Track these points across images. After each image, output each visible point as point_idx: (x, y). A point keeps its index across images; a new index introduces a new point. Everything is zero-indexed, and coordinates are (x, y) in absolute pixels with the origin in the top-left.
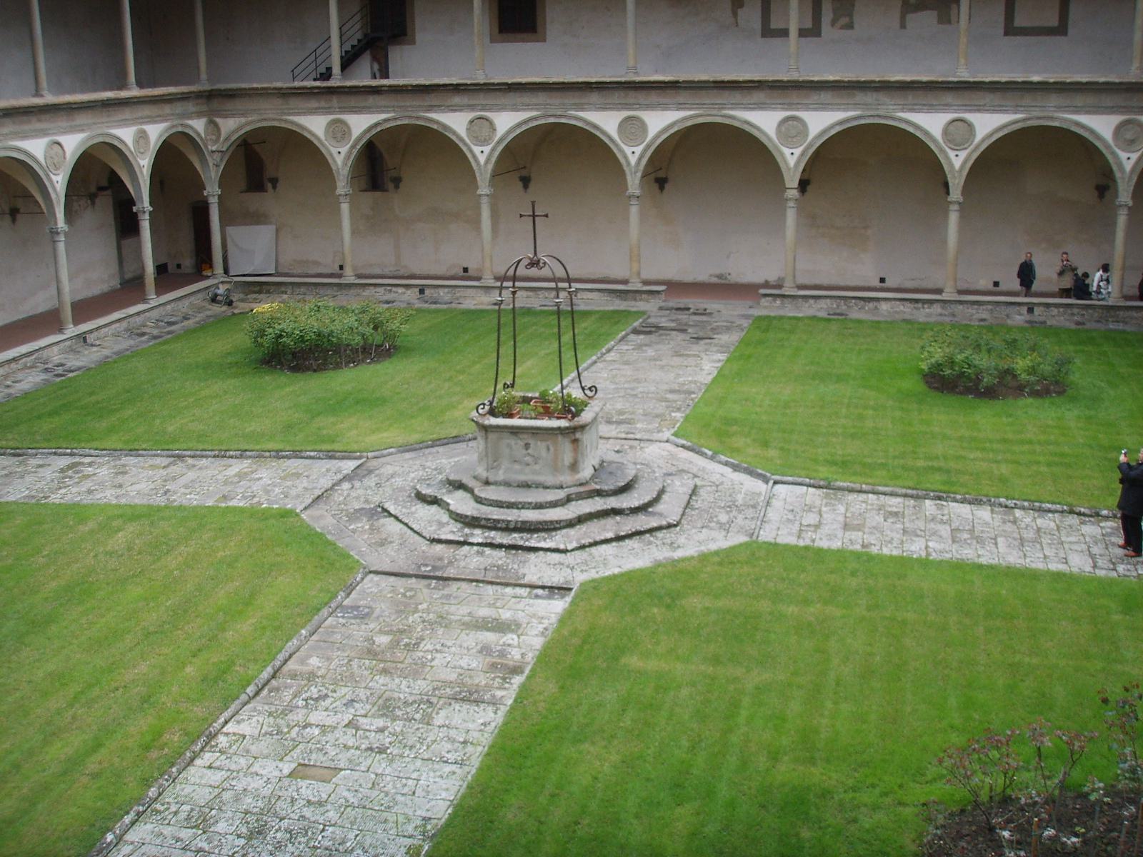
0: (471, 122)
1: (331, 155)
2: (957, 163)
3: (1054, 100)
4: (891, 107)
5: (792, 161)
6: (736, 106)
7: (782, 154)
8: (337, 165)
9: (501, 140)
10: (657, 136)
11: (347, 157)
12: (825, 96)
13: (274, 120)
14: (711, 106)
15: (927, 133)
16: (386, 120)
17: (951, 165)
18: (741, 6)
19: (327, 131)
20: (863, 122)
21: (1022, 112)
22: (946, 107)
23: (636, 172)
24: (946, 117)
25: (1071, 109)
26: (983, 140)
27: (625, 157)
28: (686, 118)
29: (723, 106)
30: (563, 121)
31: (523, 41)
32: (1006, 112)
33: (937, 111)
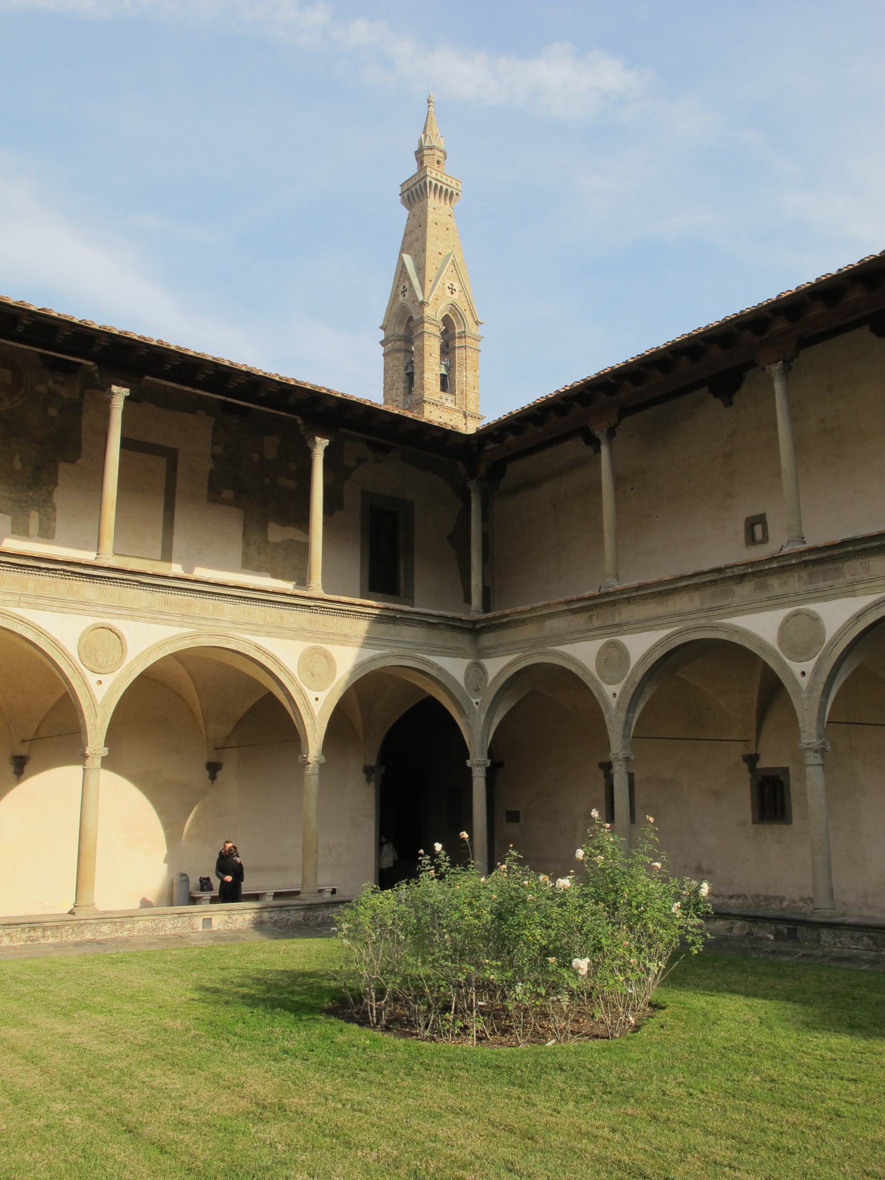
2: (100, 694)
3: (230, 610)
15: (55, 643)
17: (92, 697)
22: (84, 606)
26: (137, 659)
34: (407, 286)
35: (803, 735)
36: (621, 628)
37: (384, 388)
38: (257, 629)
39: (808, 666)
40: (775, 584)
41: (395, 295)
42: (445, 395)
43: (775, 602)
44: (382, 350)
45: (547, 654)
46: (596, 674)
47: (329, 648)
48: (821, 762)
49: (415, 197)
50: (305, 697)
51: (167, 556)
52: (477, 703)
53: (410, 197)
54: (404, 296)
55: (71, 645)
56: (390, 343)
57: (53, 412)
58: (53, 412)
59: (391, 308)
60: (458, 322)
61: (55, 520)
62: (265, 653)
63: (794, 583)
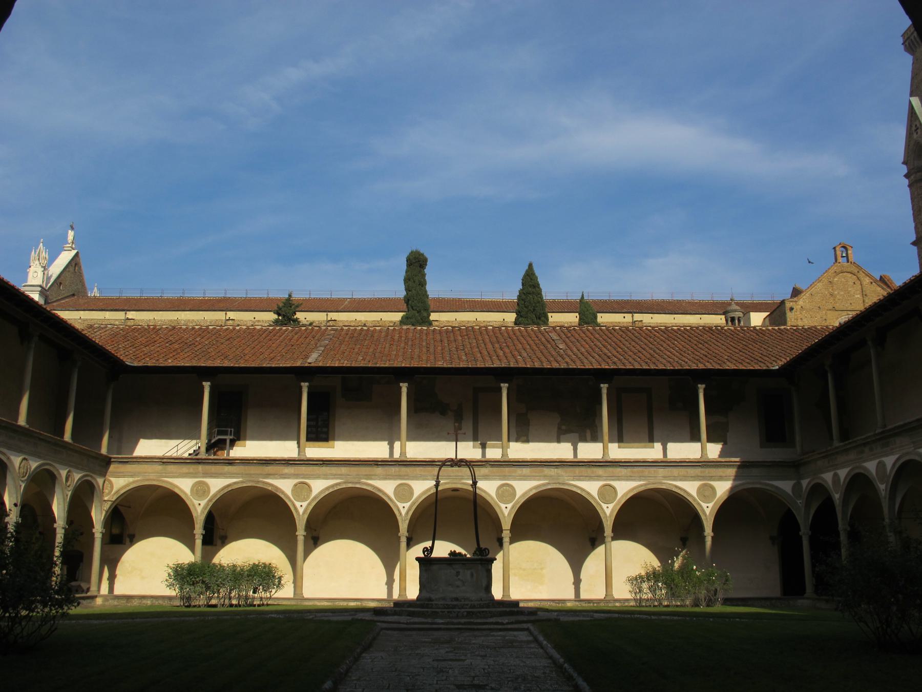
0: (295, 485)
1: (194, 505)
2: (608, 512)
4: (566, 478)
5: (506, 512)
7: (500, 507)
8: (197, 512)
9: (315, 498)
10: (419, 497)
11: (204, 508)
12: (526, 471)
13: (154, 480)
14: (454, 477)
15: (589, 493)
16: (235, 483)
17: (605, 513)
19: (192, 490)
20: (549, 487)
21: (643, 480)
22: (598, 478)
23: (405, 520)
24: (599, 484)
25: (672, 478)
26: (622, 496)
27: (399, 510)
30: (358, 486)
31: (319, 447)
32: (634, 480)
33: (594, 480)
34: (918, 125)
37: (913, 214)
38: (675, 479)
41: (910, 134)
44: (906, 182)
47: (712, 483)
49: (915, 43)
50: (701, 506)
51: (651, 440)
52: (800, 503)
53: (911, 44)
54: (917, 133)
55: (595, 493)
56: (911, 175)
59: (909, 146)
61: (597, 432)
62: (680, 488)
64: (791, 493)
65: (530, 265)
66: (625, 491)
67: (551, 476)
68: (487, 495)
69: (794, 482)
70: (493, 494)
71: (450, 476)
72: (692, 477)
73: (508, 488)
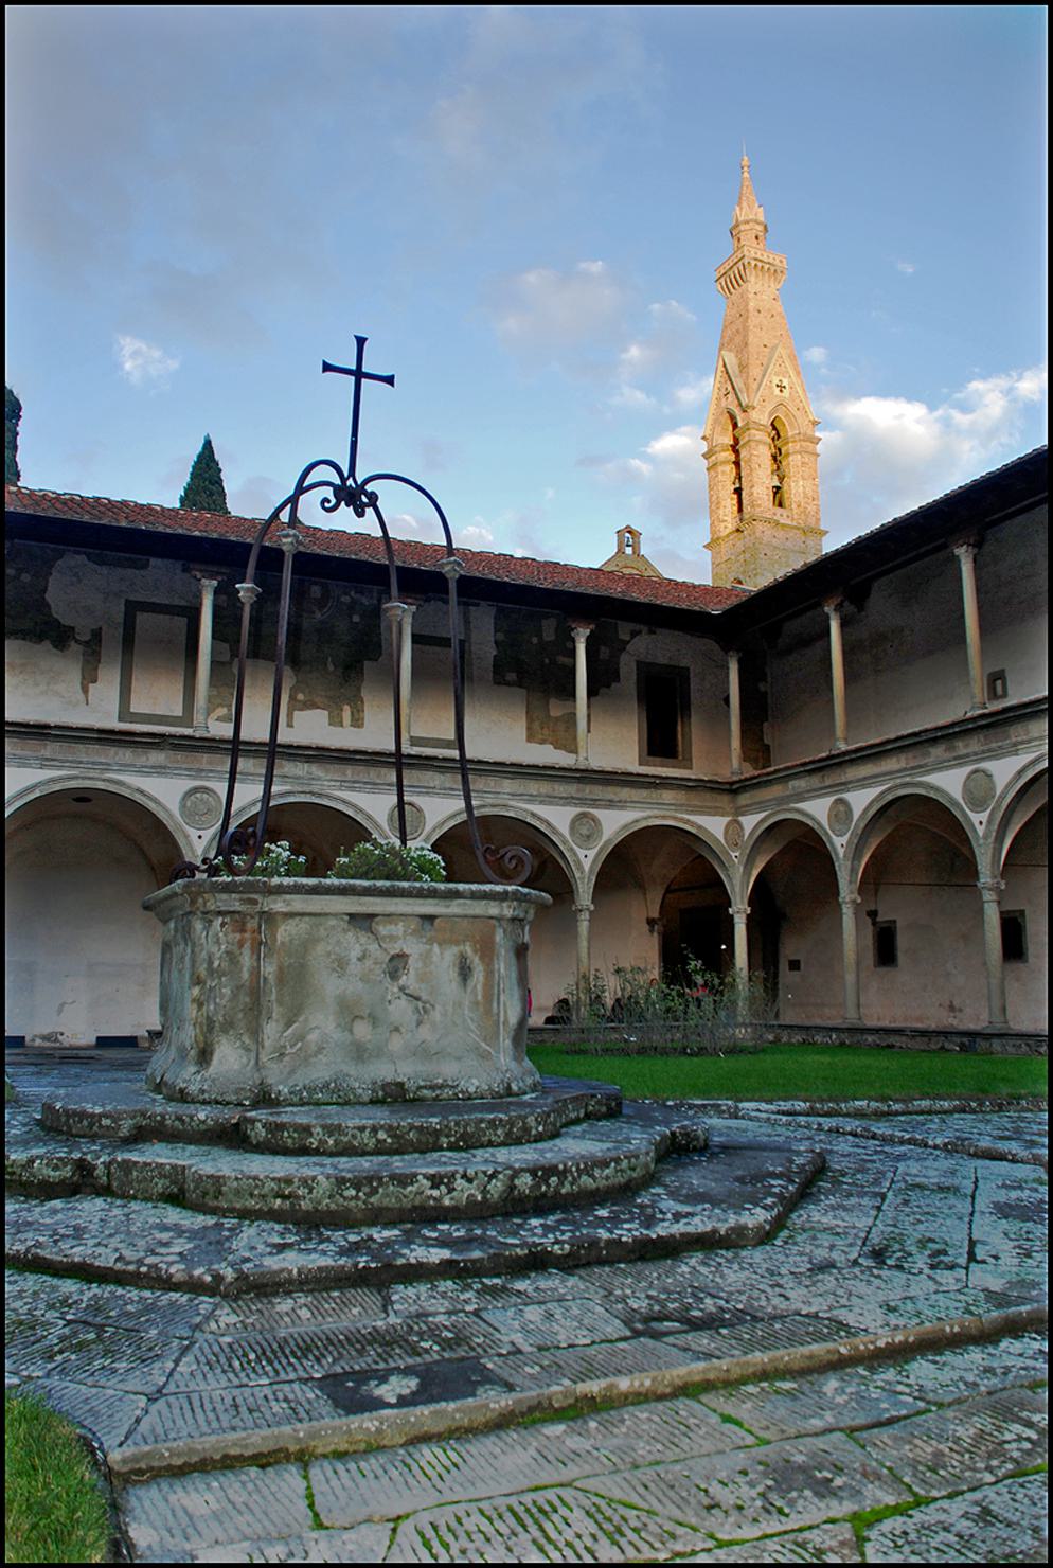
6: (125, 767)
7: (187, 836)
15: (369, 817)
18: (94, 681)
28: (53, 780)
29: (107, 767)
35: (981, 876)
36: (845, 786)
38: (532, 799)
39: (984, 816)
40: (961, 747)
42: (779, 510)
43: (961, 760)
45: (790, 810)
46: (827, 828)
48: (994, 898)
50: (575, 854)
57: (356, 619)
58: (356, 619)
60: (791, 424)
62: (539, 818)
63: (974, 744)
64: (721, 838)
65: (208, 444)
66: (440, 818)
67: (298, 778)
68: (160, 809)
69: (729, 819)
70: (174, 807)
71: (81, 762)
72: (561, 798)
73: (205, 796)
